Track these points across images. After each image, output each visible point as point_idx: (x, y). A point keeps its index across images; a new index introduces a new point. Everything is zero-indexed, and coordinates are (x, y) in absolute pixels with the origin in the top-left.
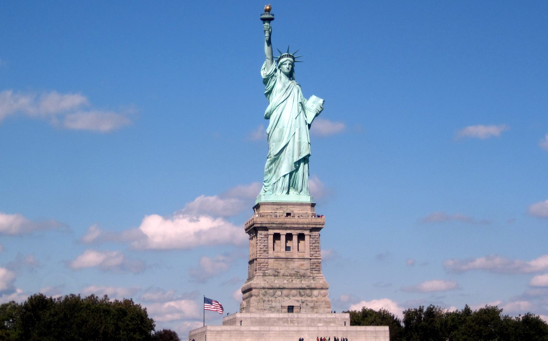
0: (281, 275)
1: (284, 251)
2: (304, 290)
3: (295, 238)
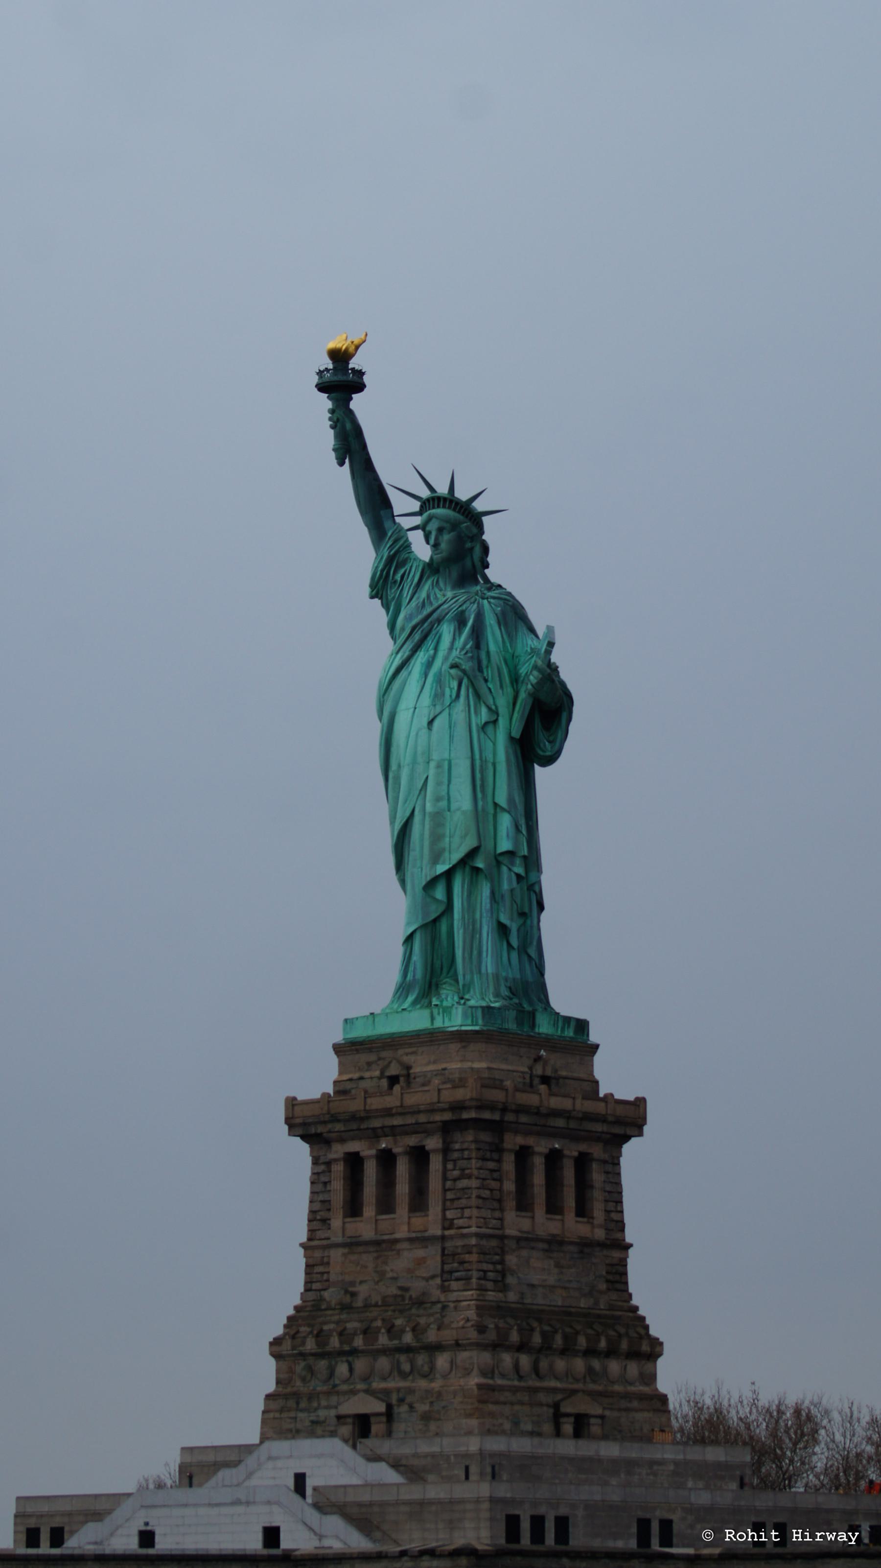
0: (359, 1303)
2: (411, 1355)
3: (403, 1168)
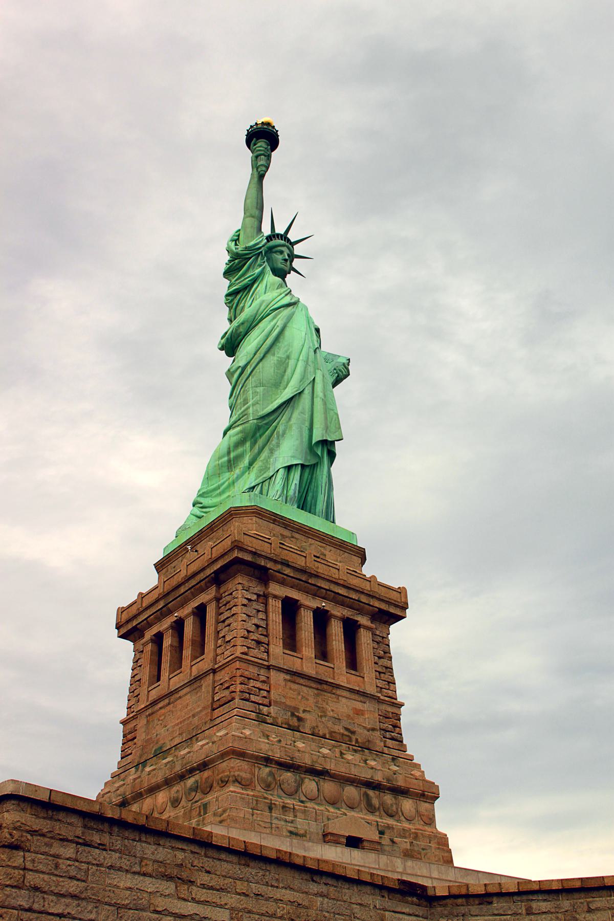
1: (311, 658)
3: (336, 630)
